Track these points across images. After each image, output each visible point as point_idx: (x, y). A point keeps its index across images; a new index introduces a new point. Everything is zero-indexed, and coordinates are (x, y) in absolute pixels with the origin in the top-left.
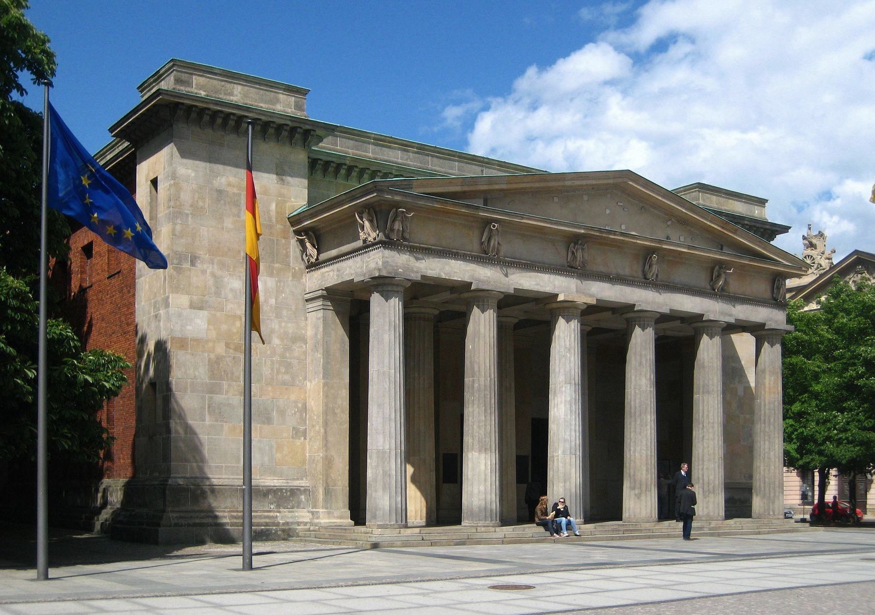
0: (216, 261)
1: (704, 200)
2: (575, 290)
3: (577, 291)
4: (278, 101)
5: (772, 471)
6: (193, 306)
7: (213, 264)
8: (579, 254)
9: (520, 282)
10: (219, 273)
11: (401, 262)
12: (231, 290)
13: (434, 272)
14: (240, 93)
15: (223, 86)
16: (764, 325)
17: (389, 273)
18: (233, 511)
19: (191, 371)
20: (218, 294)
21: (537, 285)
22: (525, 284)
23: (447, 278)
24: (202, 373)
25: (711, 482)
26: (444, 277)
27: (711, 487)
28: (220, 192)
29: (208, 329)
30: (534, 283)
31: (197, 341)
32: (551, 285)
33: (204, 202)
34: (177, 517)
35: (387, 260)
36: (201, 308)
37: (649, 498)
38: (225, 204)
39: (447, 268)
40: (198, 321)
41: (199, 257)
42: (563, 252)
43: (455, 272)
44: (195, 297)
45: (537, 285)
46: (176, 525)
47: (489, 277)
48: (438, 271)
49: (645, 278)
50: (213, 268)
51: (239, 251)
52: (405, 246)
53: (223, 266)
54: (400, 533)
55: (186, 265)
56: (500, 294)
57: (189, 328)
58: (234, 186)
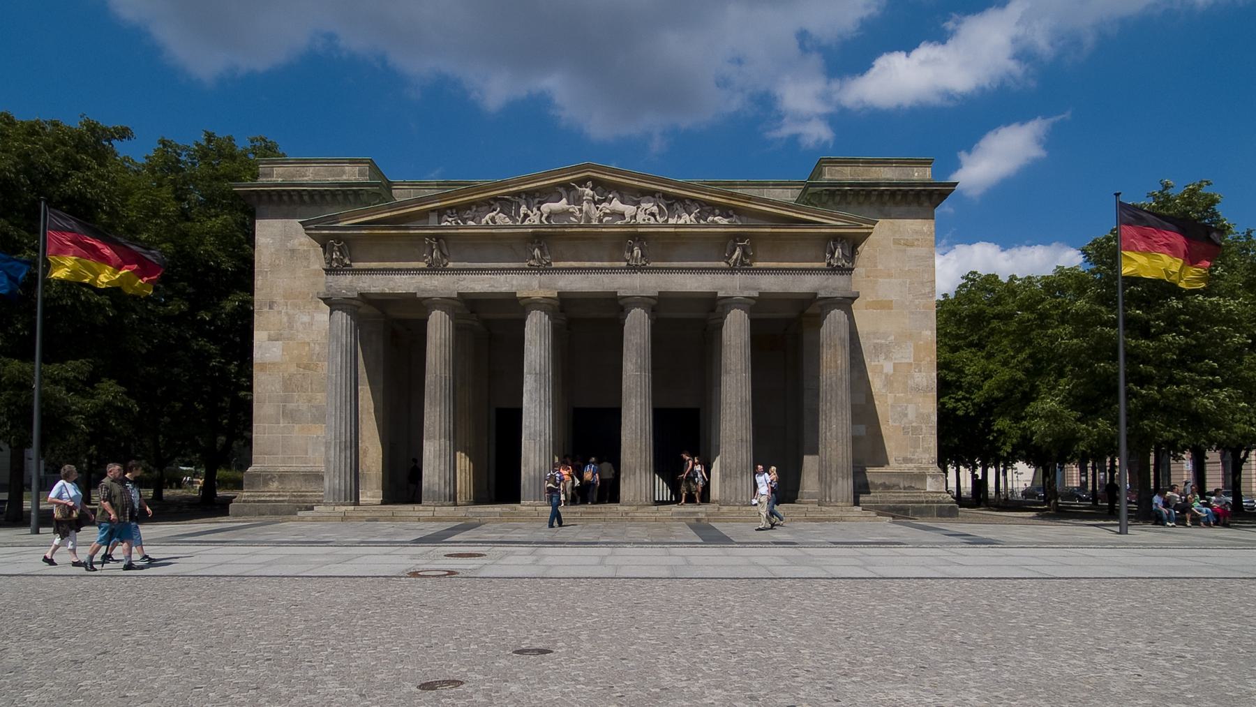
1: (831, 175)
3: (540, 287)
4: (344, 173)
5: (828, 454)
6: (269, 339)
7: (287, 305)
9: (471, 286)
10: (291, 312)
12: (302, 323)
13: (377, 288)
16: (816, 294)
18: (295, 492)
19: (269, 387)
20: (291, 327)
21: (490, 287)
22: (476, 288)
23: (391, 292)
24: (278, 386)
25: (728, 465)
26: (387, 291)
27: (728, 470)
28: (293, 251)
29: (283, 354)
31: (274, 364)
34: (248, 496)
36: (277, 340)
37: (632, 481)
38: (297, 260)
39: (391, 284)
40: (275, 349)
41: (276, 302)
43: (399, 286)
44: (272, 332)
46: (244, 501)
47: (436, 286)
48: (381, 288)
50: (287, 308)
51: (308, 294)
52: (347, 270)
53: (295, 306)
54: (334, 510)
56: (651, 300)
57: (267, 355)
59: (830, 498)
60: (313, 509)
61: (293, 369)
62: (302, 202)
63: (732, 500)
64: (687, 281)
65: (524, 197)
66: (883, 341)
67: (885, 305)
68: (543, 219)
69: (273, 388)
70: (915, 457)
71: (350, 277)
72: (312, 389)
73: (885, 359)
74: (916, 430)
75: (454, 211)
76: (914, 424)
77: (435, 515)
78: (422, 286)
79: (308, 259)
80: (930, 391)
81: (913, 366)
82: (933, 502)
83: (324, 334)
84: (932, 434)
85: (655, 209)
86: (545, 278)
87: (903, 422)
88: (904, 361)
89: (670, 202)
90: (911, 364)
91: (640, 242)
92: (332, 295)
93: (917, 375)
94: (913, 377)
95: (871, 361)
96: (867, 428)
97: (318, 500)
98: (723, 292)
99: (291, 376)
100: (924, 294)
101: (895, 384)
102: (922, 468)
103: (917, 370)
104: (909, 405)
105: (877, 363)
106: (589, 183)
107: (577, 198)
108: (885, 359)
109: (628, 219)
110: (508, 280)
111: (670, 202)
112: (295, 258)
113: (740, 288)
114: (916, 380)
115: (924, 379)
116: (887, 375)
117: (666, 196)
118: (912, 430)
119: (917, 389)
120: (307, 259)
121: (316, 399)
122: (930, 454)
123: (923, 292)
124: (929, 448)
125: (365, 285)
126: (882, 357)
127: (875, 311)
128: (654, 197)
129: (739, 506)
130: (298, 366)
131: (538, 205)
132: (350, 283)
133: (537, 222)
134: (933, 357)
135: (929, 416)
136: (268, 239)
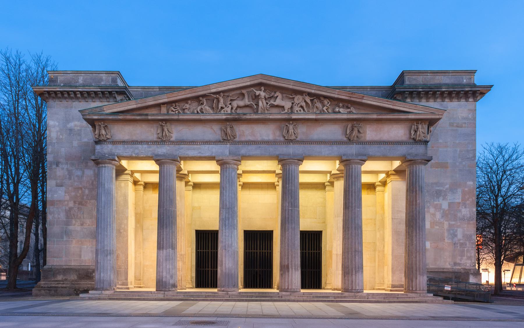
0: (69, 163)
2: (228, 153)
3: (230, 153)
8: (229, 130)
9: (187, 153)
11: (107, 151)
14: (82, 81)
15: (73, 79)
17: (96, 158)
22: (190, 154)
28: (71, 130)
30: (197, 152)
32: (209, 152)
33: (63, 136)
35: (98, 151)
38: (73, 135)
39: (136, 151)
42: (219, 132)
43: (142, 152)
45: (200, 153)
49: (287, 140)
52: (109, 142)
55: (54, 166)
58: (78, 126)
59: (412, 288)
61: (71, 204)
62: (76, 98)
63: (350, 289)
64: (322, 150)
66: (441, 188)
67: (443, 166)
68: (233, 111)
69: (59, 216)
70: (462, 262)
71: (110, 146)
72: (83, 217)
73: (443, 200)
74: (462, 244)
76: (461, 241)
77: (165, 296)
78: (156, 152)
79: (80, 135)
81: (461, 205)
83: (91, 183)
84: (473, 247)
86: (233, 147)
87: (454, 240)
88: (457, 201)
90: (459, 203)
91: (293, 125)
92: (100, 158)
94: (460, 211)
95: (434, 201)
97: (88, 287)
98: (346, 157)
99: (71, 209)
100: (468, 158)
101: (449, 216)
102: (466, 269)
103: (463, 207)
104: (459, 229)
107: (254, 97)
108: (443, 200)
109: (286, 111)
110: (210, 149)
112: (72, 135)
113: (355, 155)
114: (463, 213)
115: (468, 213)
116: (444, 210)
118: (460, 245)
119: (463, 219)
120: (80, 135)
121: (86, 224)
122: (471, 260)
123: (468, 157)
124: (471, 256)
125: (120, 151)
126: (441, 198)
127: (437, 169)
129: (354, 292)
130: (75, 202)
131: (230, 102)
132: (111, 150)
133: (229, 112)
134: (474, 198)
135: (471, 236)
136: (56, 122)
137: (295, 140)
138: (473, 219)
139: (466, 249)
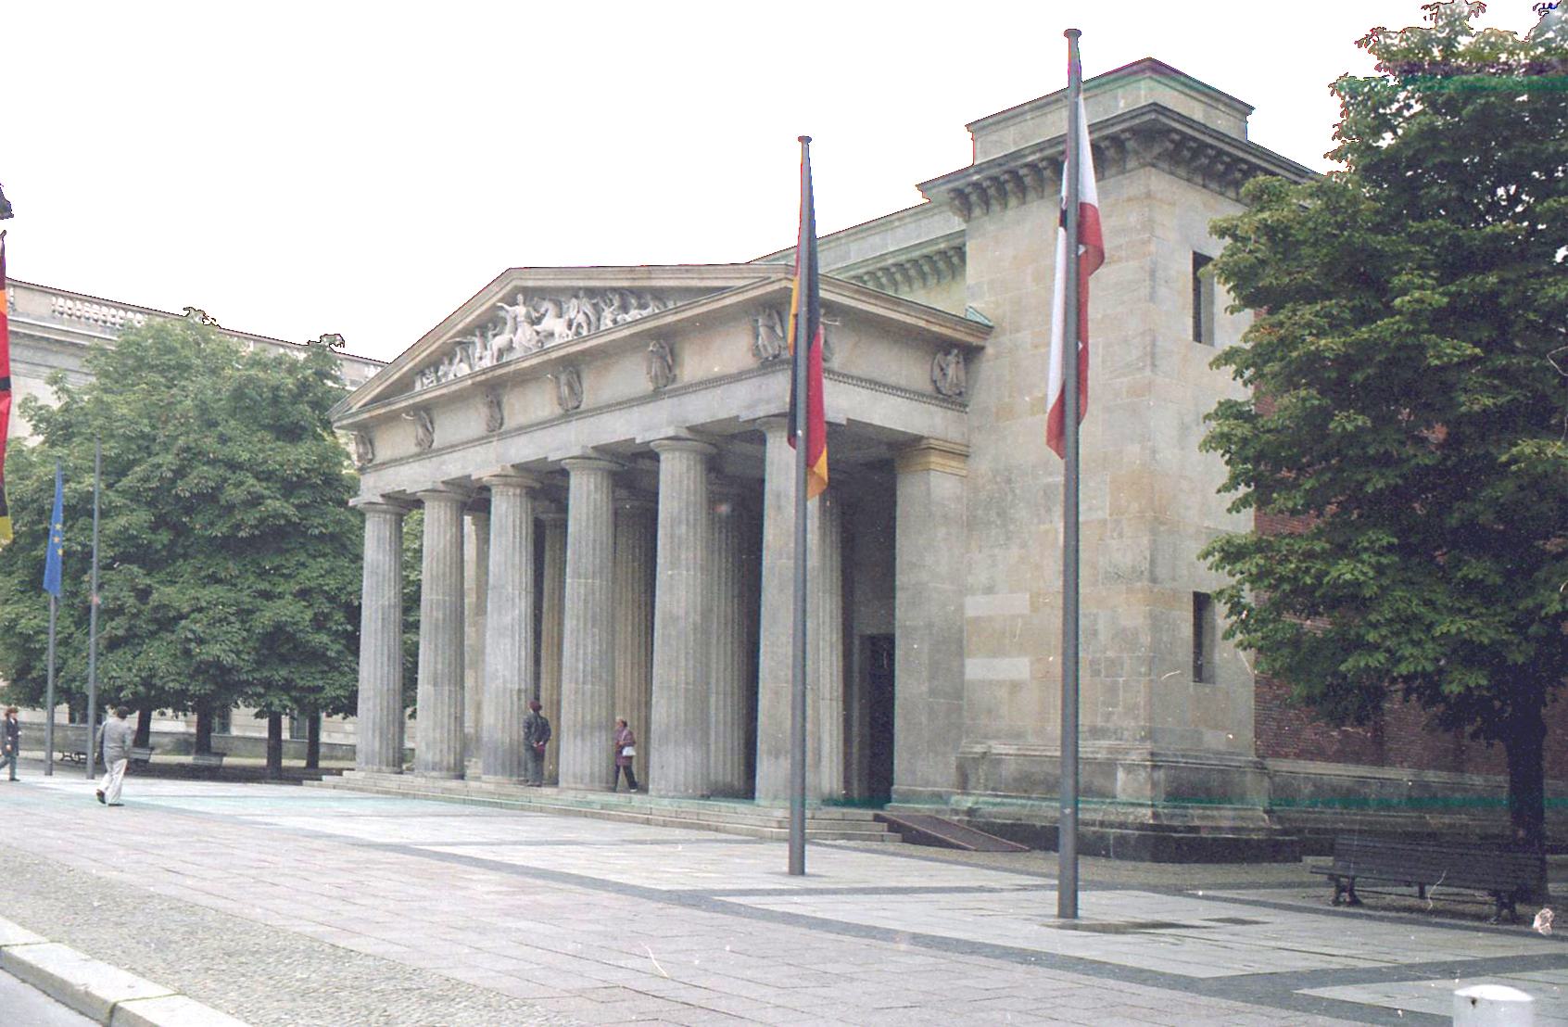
60: (340, 774)
65: (478, 333)
71: (374, 474)
75: (432, 369)
76: (1110, 654)
80: (1139, 579)
82: (1111, 825)
85: (581, 318)
89: (595, 301)
90: (1105, 521)
93: (1114, 543)
96: (1032, 664)
103: (1115, 535)
105: (1047, 526)
106: (520, 298)
111: (595, 301)
117: (591, 292)
122: (1136, 718)
128: (577, 297)
137: (577, 407)
138: (1142, 572)
139: (1121, 680)
